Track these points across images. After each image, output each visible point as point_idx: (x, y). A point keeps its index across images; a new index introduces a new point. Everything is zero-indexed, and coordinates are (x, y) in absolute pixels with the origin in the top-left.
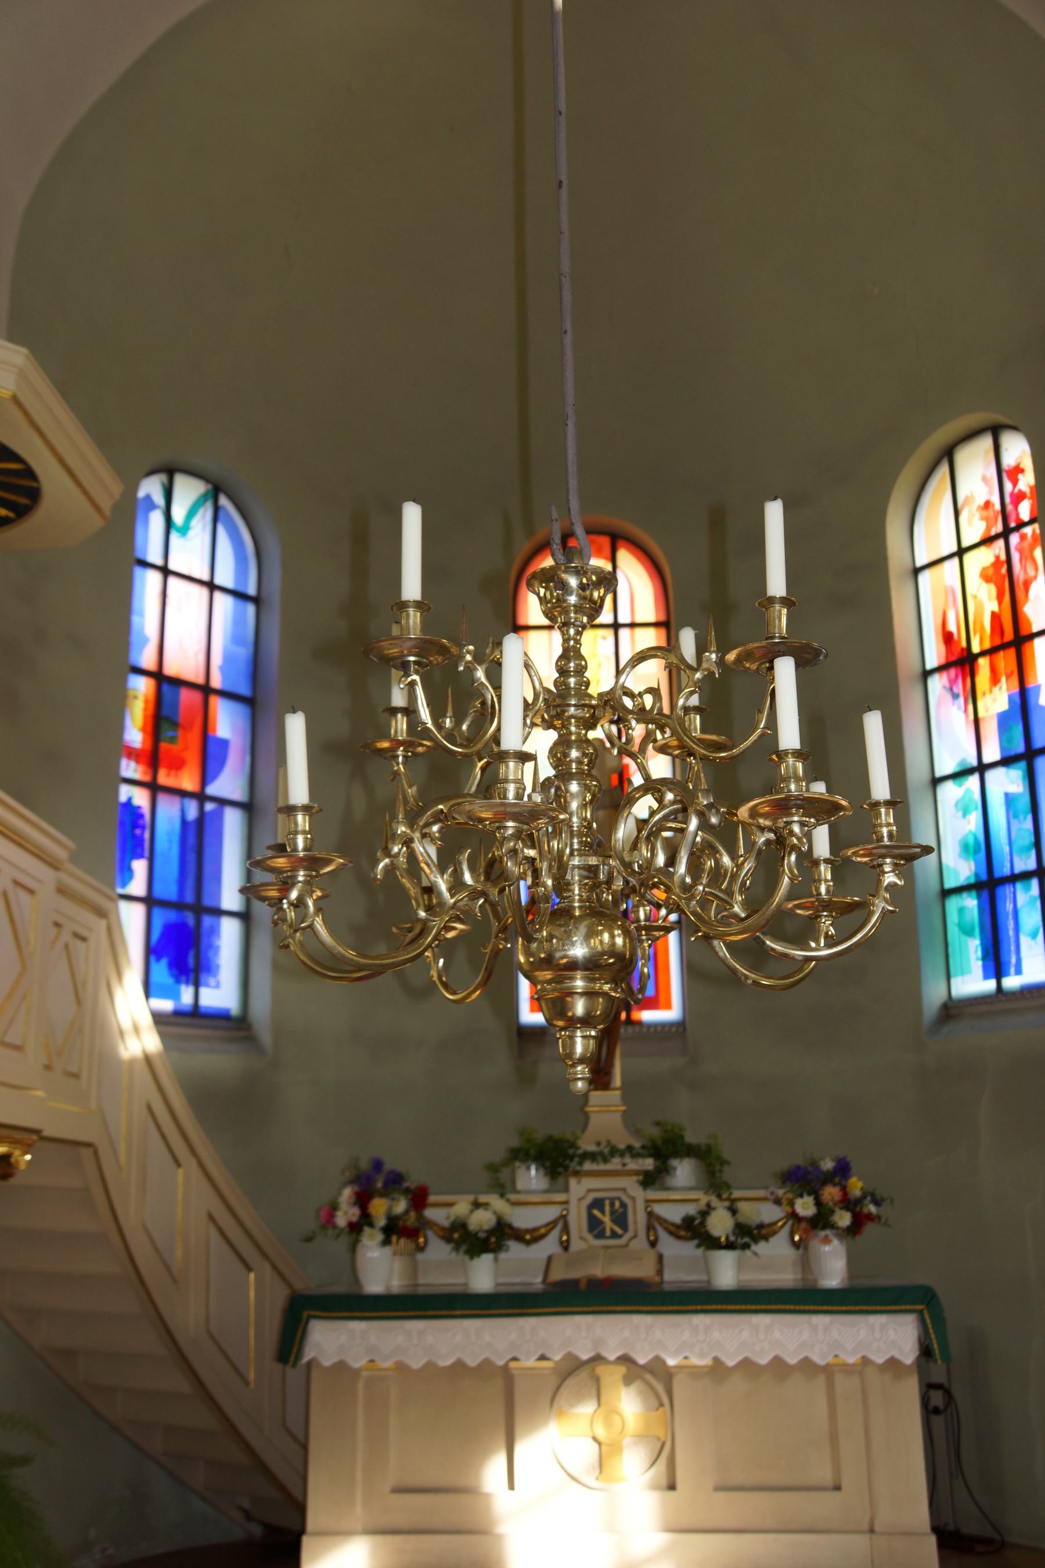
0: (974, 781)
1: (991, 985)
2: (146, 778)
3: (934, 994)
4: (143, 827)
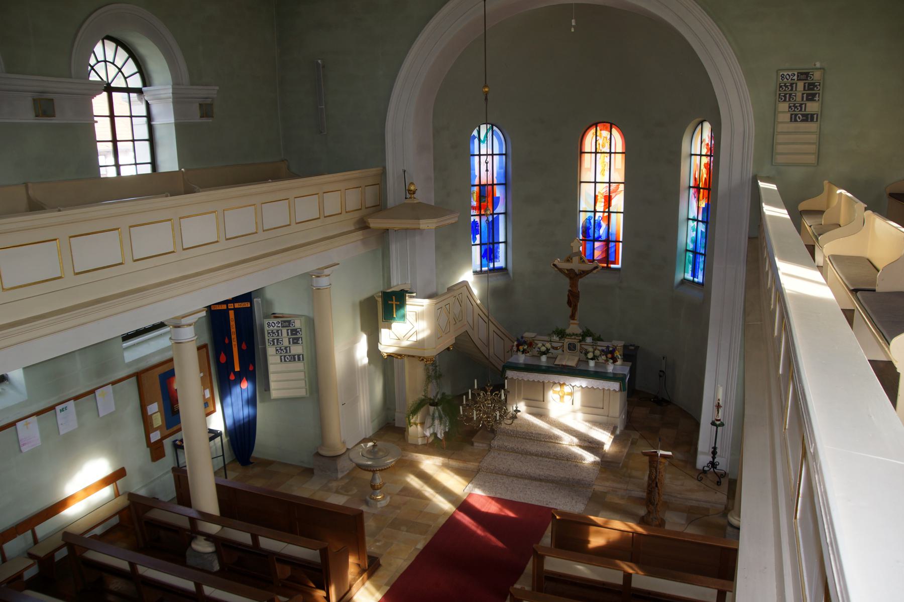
0: (696, 223)
1: (692, 278)
2: (478, 213)
3: (679, 277)
4: (478, 226)
